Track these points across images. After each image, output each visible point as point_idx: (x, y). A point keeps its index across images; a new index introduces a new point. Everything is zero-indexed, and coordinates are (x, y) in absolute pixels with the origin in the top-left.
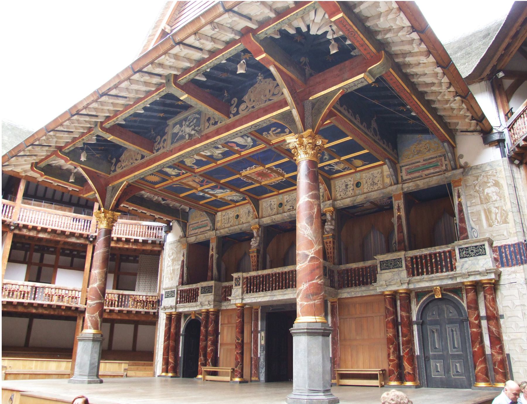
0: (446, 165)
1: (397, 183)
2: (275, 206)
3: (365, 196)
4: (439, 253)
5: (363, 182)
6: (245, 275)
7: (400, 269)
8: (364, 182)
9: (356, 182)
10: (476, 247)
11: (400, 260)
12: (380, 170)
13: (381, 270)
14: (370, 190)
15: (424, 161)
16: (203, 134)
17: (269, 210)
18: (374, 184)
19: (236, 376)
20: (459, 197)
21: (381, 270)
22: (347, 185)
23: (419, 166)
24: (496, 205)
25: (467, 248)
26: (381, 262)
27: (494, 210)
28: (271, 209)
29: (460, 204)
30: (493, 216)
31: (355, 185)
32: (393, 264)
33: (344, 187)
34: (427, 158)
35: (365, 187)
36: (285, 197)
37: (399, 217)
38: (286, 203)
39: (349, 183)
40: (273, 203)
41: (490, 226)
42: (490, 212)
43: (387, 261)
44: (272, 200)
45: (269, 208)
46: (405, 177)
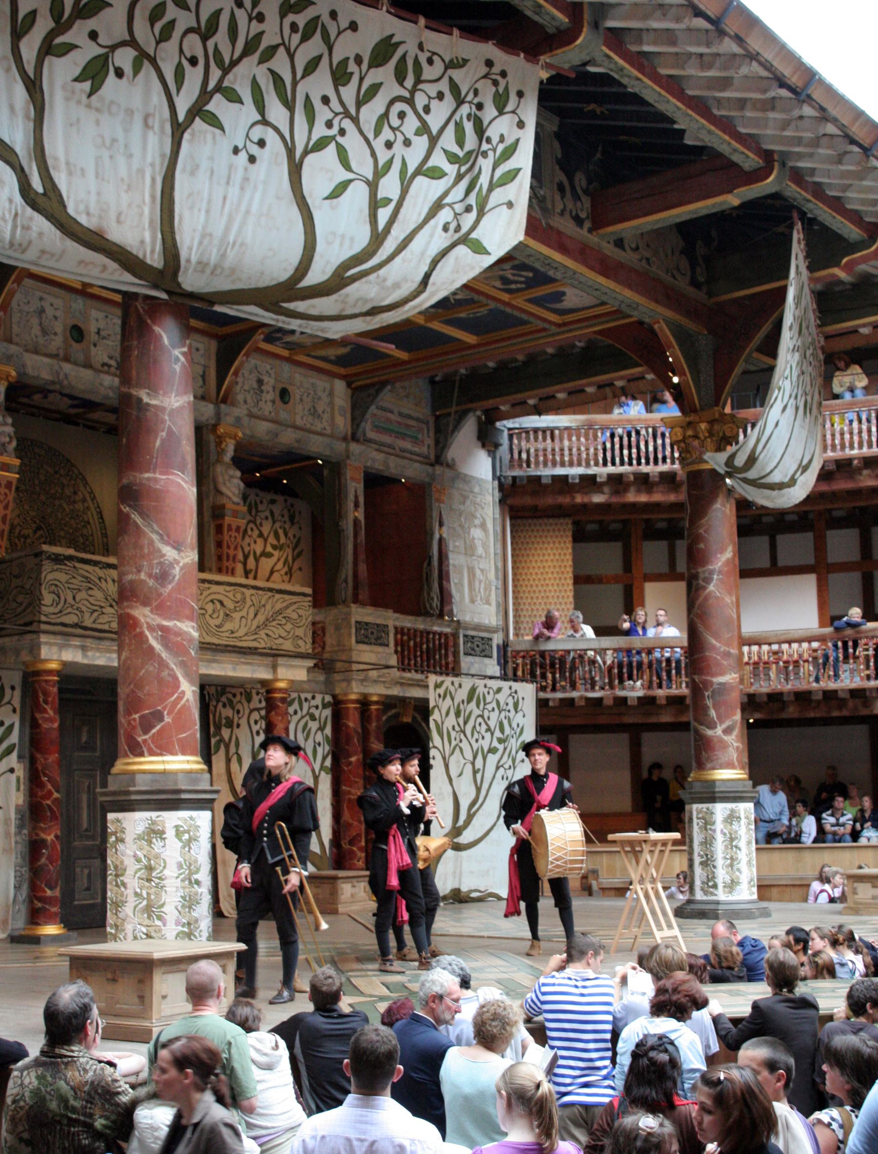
0: (429, 446)
1: (354, 438)
2: (59, 327)
3: (299, 434)
4: (434, 633)
5: (296, 393)
6: (408, 622)
7: (386, 649)
8: (298, 397)
9: (280, 386)
10: (483, 638)
11: (383, 628)
12: (327, 385)
13: (357, 642)
14: (308, 426)
15: (400, 414)
16: (552, 223)
17: (36, 330)
18: (314, 413)
19: (50, 919)
20: (441, 525)
21: (357, 642)
22: (260, 382)
23: (389, 420)
24: (482, 567)
25: (473, 637)
26: (357, 622)
27: (478, 573)
28: (45, 332)
29: (441, 540)
30: (477, 584)
31: (278, 393)
32: (375, 636)
33: (255, 385)
34: (406, 411)
35: (299, 413)
36: (94, 313)
37: (356, 521)
38: (94, 337)
39: (266, 379)
40: (50, 312)
41: (473, 601)
42: (474, 575)
43: (367, 624)
44: (50, 299)
45: (35, 321)
46: (371, 435)
